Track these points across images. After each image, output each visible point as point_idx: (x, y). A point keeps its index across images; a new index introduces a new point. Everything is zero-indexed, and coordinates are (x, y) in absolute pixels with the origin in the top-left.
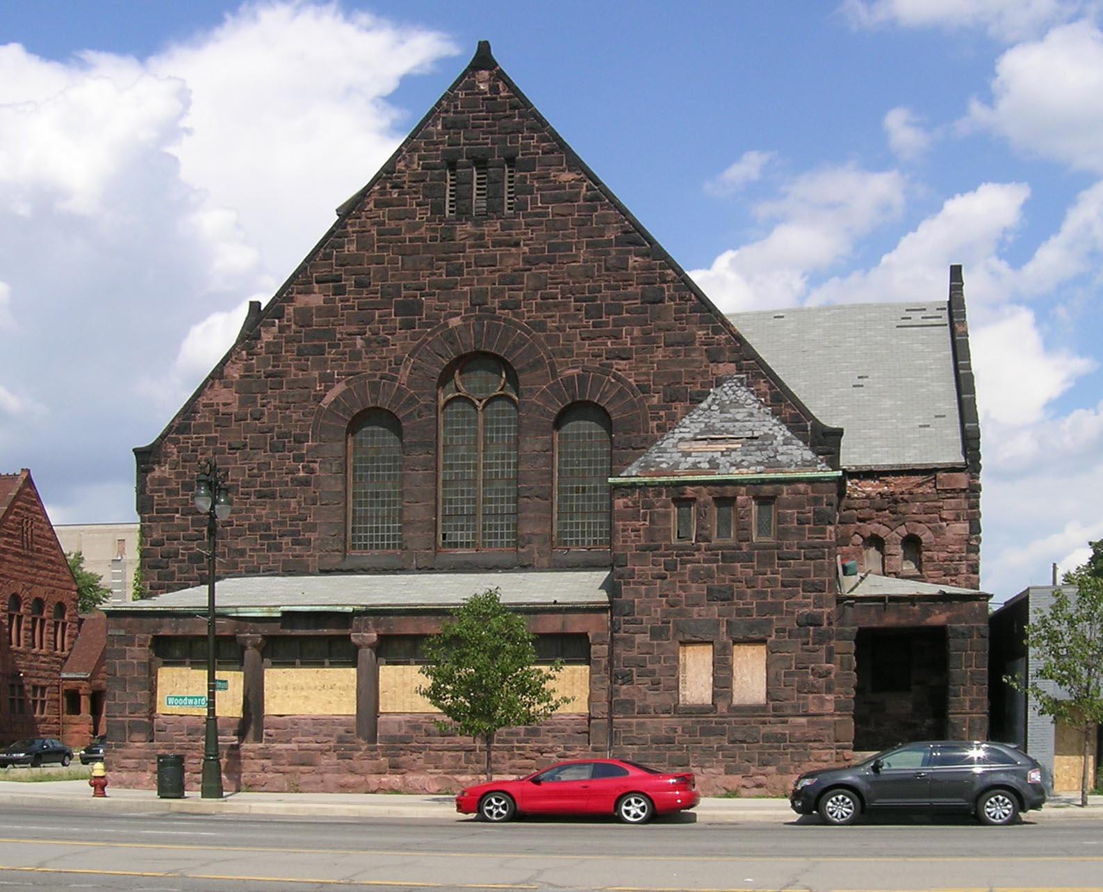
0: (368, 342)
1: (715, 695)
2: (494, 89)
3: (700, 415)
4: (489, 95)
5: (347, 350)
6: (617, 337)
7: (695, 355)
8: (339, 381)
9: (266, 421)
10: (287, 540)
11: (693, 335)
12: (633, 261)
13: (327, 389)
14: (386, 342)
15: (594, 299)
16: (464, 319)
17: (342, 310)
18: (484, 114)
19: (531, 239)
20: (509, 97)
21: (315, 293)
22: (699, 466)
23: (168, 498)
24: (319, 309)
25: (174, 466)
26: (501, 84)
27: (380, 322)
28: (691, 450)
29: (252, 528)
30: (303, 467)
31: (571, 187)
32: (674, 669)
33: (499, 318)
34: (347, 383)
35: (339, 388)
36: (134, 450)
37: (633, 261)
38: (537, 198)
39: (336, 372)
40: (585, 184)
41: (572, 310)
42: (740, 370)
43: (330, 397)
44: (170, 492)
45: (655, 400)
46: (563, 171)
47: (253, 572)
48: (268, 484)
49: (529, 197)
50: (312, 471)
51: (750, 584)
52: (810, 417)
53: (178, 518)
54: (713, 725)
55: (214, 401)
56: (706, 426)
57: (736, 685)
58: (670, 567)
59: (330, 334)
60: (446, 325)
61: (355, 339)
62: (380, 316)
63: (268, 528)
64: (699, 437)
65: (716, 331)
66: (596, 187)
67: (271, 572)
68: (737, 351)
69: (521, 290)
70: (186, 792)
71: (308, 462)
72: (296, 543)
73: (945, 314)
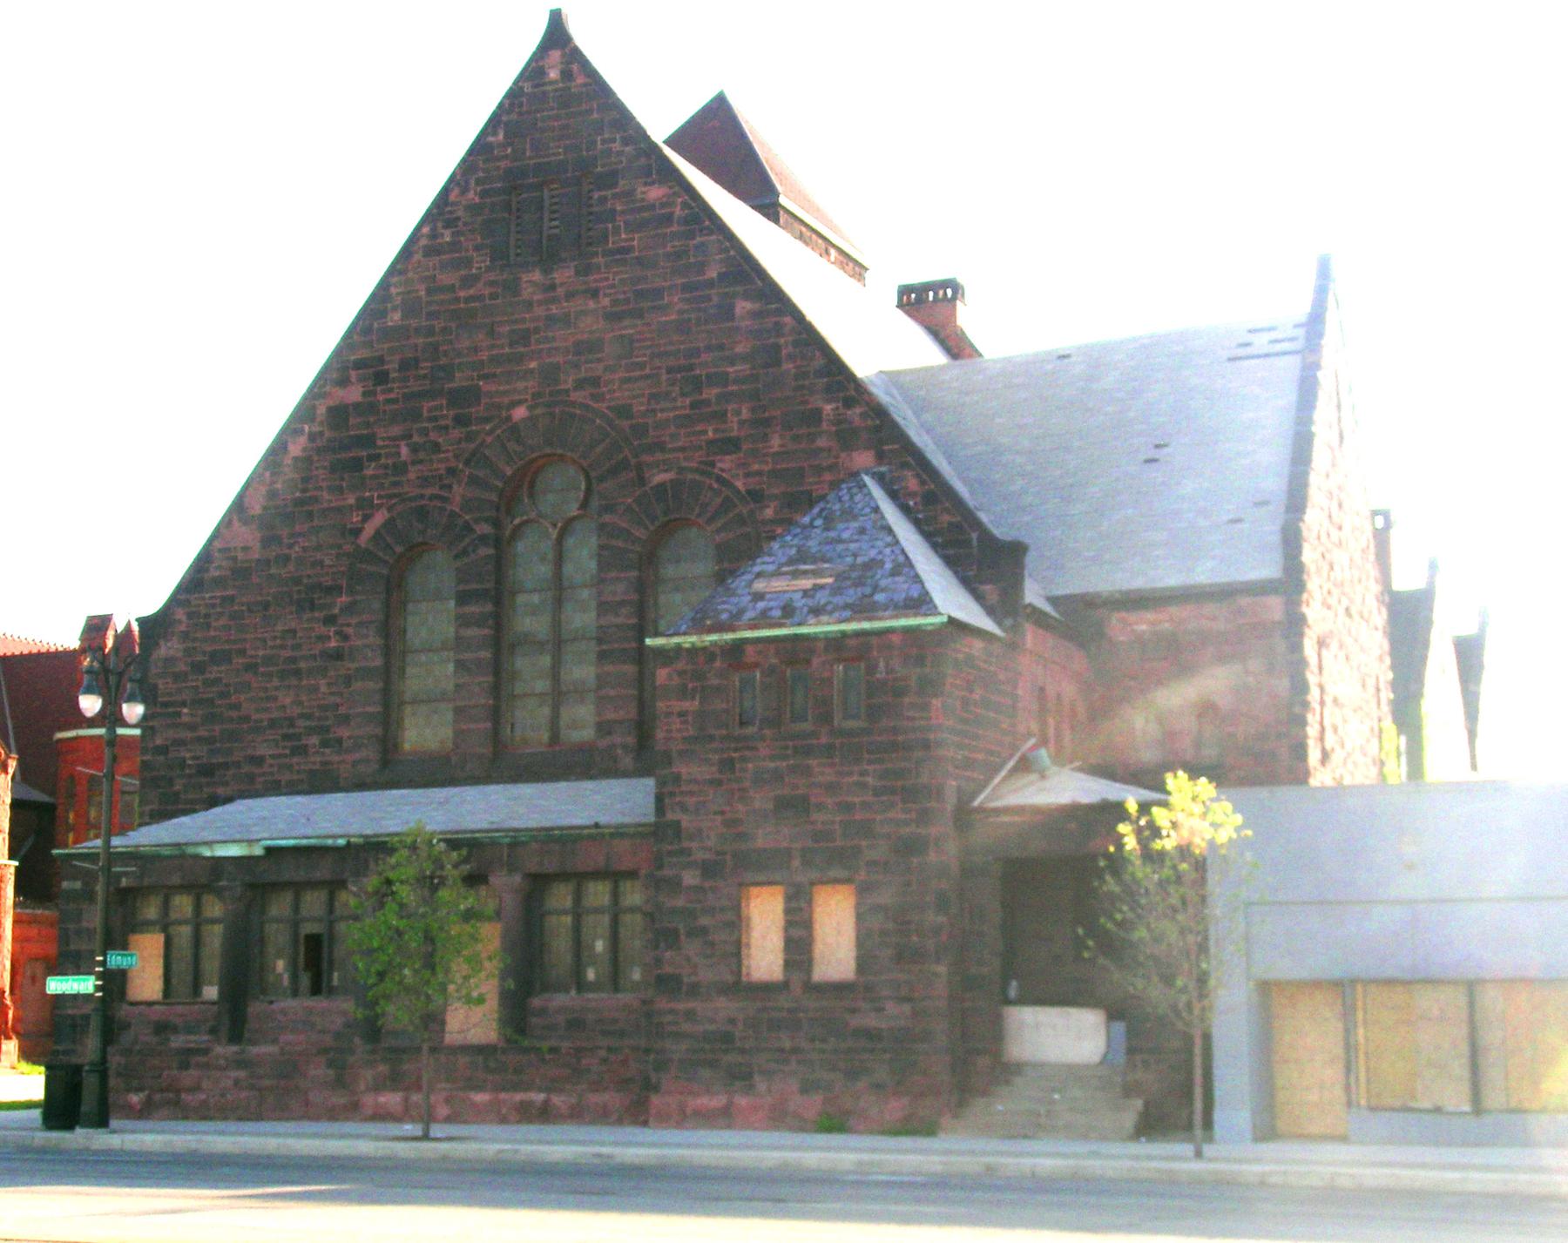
0: (415, 449)
1: (788, 964)
2: (567, 75)
3: (795, 536)
4: (561, 85)
5: (390, 462)
6: (721, 416)
7: (822, 442)
8: (381, 506)
9: (293, 570)
10: (314, 740)
11: (818, 412)
12: (743, 306)
13: (366, 518)
14: (436, 447)
15: (691, 368)
16: (530, 408)
17: (384, 404)
18: (555, 112)
19: (613, 286)
20: (586, 85)
21: (353, 384)
22: (769, 614)
23: (175, 686)
24: (356, 406)
25: (185, 636)
26: (575, 67)
27: (430, 419)
28: (767, 590)
29: (273, 723)
30: (337, 633)
31: (663, 205)
32: (736, 923)
33: (573, 404)
34: (389, 509)
35: (379, 519)
36: (137, 620)
37: (743, 306)
38: (620, 226)
39: (376, 495)
40: (680, 200)
41: (664, 384)
42: (880, 457)
43: (369, 529)
44: (177, 677)
45: (769, 513)
46: (653, 183)
47: (275, 788)
48: (293, 660)
49: (610, 226)
50: (346, 637)
51: (831, 788)
52: (978, 525)
53: (186, 714)
54: (785, 1014)
55: (232, 545)
56: (798, 551)
57: (819, 949)
58: (728, 765)
59: (369, 441)
60: (509, 418)
61: (398, 446)
62: (430, 410)
63: (291, 722)
64: (785, 569)
65: (849, 403)
66: (693, 205)
67: (293, 789)
68: (878, 429)
69: (599, 360)
70: (38, 1093)
71: (342, 625)
72: (325, 744)
73: (1301, 332)
